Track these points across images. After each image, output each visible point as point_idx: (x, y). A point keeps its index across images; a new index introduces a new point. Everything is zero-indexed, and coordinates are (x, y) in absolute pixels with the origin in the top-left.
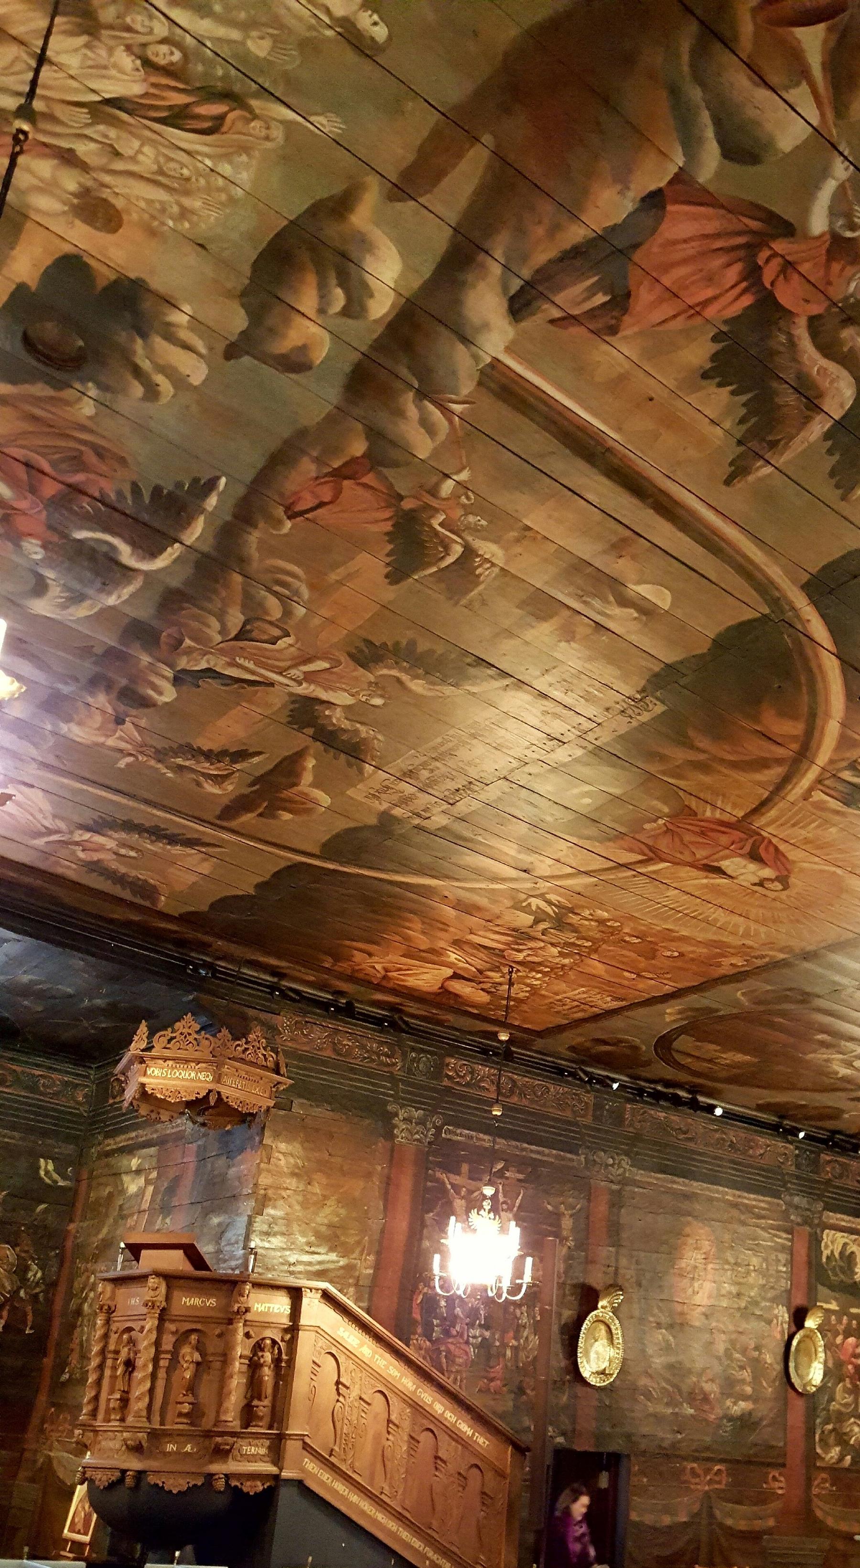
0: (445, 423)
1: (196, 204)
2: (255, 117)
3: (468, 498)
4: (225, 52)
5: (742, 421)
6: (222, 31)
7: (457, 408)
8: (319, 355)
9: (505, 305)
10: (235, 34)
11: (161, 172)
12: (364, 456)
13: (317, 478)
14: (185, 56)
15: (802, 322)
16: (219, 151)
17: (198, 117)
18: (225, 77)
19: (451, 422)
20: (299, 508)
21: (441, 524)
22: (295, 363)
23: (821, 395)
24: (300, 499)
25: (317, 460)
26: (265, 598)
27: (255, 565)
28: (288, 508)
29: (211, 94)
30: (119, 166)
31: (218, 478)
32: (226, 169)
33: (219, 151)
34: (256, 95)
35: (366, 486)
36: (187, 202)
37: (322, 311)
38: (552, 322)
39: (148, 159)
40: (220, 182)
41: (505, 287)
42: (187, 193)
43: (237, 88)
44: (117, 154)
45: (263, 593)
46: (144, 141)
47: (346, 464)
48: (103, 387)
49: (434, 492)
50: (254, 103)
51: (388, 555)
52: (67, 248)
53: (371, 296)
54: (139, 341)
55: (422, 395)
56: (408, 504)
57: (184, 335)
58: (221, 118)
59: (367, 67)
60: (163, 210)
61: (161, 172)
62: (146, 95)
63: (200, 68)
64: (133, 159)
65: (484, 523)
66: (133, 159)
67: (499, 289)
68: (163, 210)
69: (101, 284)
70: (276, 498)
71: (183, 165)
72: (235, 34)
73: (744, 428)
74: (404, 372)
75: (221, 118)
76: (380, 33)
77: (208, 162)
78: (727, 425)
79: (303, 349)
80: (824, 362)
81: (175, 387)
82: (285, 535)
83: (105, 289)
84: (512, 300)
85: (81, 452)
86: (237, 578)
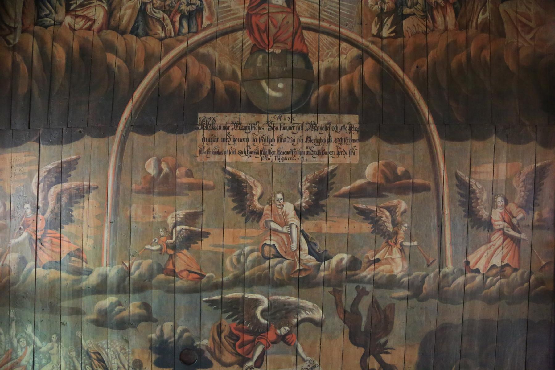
0: (134, 263)
1: (118, 348)
2: (88, 347)
3: (155, 240)
4: (80, 359)
5: (77, 202)
6: (76, 362)
7: (127, 264)
8: (138, 303)
9: (90, 275)
10: (75, 359)
11: (116, 358)
12: (163, 273)
13: (181, 279)
14: (87, 365)
15: (46, 216)
16: (102, 350)
17: (97, 357)
18: (85, 356)
19: (133, 263)
20: (197, 276)
21: (172, 239)
22: (146, 306)
23: (58, 194)
24: (194, 278)
25: (174, 281)
26: (249, 261)
27: (236, 272)
28: (201, 279)
29: (90, 357)
30: (121, 366)
31: (205, 301)
32: (105, 346)
33: (102, 350)
34: (84, 349)
35: (174, 265)
36: (119, 350)
37: (124, 310)
38: (86, 263)
39: (115, 361)
40: (109, 346)
41: (86, 278)
42: (117, 351)
43: (85, 353)
44: (119, 367)
45: (248, 262)
46: (112, 364)
47: (170, 275)
48: (194, 342)
49: (161, 249)
50: (86, 349)
51: (197, 243)
52: (153, 366)
53: (112, 303)
54: (169, 341)
55: (129, 274)
56: (171, 252)
57: (158, 332)
58: (94, 353)
59: (62, 334)
60: (125, 353)
61: (116, 358)
62: (100, 368)
63: (86, 361)
64: (117, 364)
65: (161, 230)
66: (117, 364)
67: (88, 280)
68: (125, 353)
69: (158, 356)
70: (199, 283)
71: (111, 355)
72: (75, 359)
73: (78, 200)
74: (126, 283)
75: (94, 353)
76: (54, 336)
77: (107, 350)
78: (81, 204)
79: (140, 307)
80: (50, 203)
81: (178, 326)
82: (213, 273)
83: (159, 354)
84: (89, 275)
85: (225, 337)
86: (247, 273)
